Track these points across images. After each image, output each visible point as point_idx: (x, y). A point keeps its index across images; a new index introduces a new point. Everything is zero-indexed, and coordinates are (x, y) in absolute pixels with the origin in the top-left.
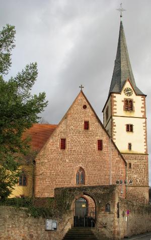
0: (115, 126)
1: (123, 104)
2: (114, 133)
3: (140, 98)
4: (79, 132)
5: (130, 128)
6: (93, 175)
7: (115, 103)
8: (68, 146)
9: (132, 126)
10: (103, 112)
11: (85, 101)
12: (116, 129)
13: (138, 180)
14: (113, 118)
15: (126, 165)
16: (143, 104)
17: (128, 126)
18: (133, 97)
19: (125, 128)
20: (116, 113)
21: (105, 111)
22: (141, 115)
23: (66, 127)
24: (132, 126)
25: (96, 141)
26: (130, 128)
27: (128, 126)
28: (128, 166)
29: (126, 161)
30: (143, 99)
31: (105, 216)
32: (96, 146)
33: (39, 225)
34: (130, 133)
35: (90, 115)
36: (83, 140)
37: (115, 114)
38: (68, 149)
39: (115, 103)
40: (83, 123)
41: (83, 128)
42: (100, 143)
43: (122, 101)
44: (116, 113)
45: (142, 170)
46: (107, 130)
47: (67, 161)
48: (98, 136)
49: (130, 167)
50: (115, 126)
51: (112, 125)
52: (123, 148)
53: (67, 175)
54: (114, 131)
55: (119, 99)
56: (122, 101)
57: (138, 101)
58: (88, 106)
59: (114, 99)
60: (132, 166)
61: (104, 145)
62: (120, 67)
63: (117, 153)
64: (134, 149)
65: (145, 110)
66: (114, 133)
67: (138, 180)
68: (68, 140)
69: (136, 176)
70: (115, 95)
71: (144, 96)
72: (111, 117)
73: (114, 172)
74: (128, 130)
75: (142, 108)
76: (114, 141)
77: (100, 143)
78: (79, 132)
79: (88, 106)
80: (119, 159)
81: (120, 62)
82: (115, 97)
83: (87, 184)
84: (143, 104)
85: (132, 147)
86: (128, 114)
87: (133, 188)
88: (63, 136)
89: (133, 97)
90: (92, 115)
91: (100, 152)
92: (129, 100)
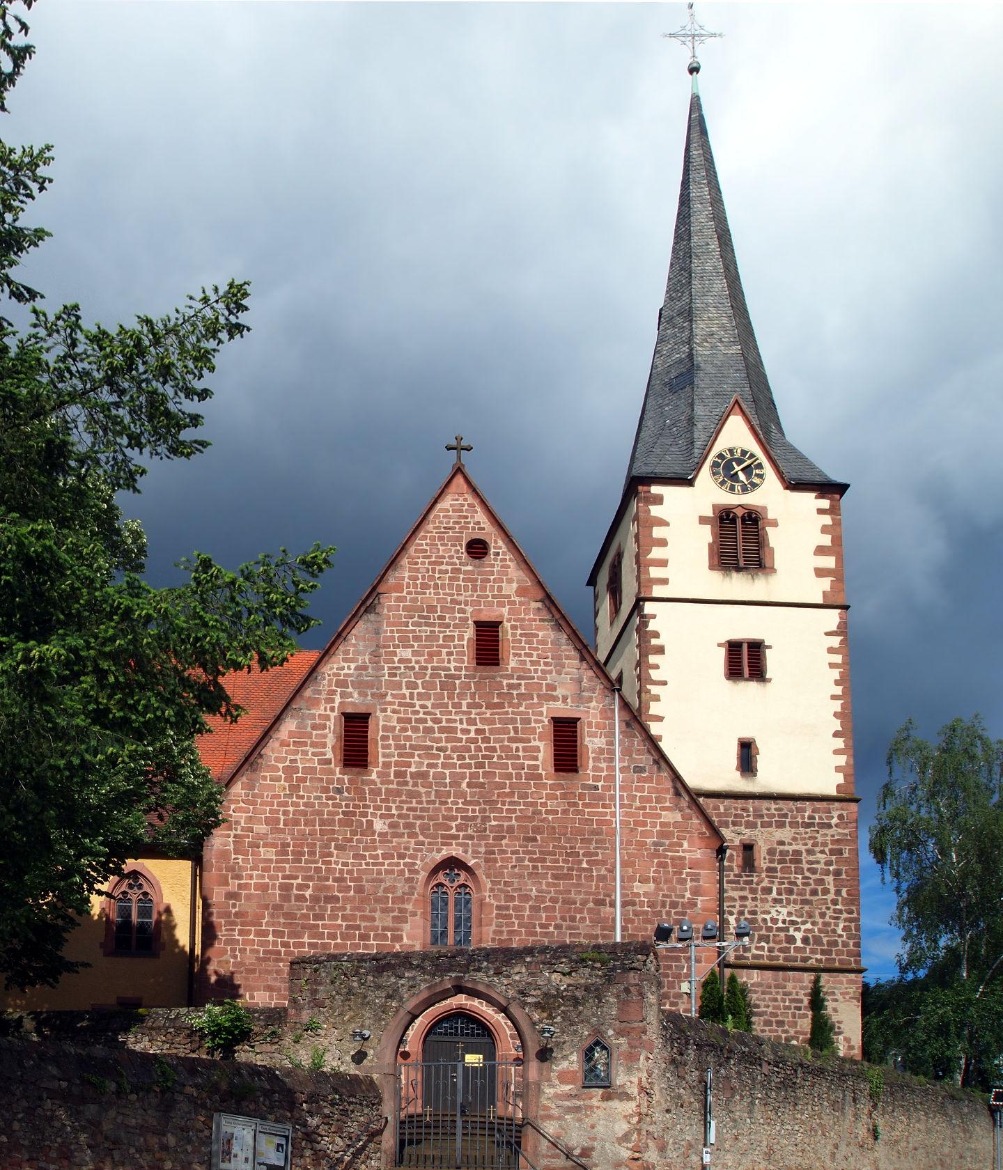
0: (660, 650)
1: (706, 535)
2: (654, 690)
3: (809, 501)
4: (447, 685)
5: (746, 661)
6: (526, 898)
7: (657, 532)
8: (382, 751)
9: (757, 648)
10: (592, 581)
11: (481, 516)
12: (663, 667)
13: (799, 936)
14: (649, 608)
15: (721, 851)
16: (825, 530)
17: (733, 648)
18: (769, 495)
19: (719, 657)
20: (664, 581)
21: (604, 578)
22: (817, 589)
23: (375, 655)
24: (757, 648)
25: (542, 724)
26: (746, 661)
27: (733, 648)
28: (734, 859)
29: (725, 832)
30: (825, 504)
31: (577, 1109)
32: (544, 751)
33: (171, 1140)
34: (750, 688)
35: (510, 589)
36: (471, 722)
37: (657, 591)
38: (387, 765)
39: (657, 532)
40: (470, 633)
41: (468, 659)
42: (565, 736)
43: (703, 520)
44: (664, 581)
45: (821, 882)
46: (614, 675)
47: (379, 825)
48: (555, 699)
49: (749, 863)
50: (660, 650)
51: (648, 646)
52: (709, 767)
53: (378, 900)
54: (654, 674)
55: (682, 516)
56: (703, 520)
57: (795, 524)
58: (497, 545)
59: (655, 511)
60: (762, 862)
61: (591, 742)
62: (690, 340)
63: (669, 785)
64: (773, 775)
65: (839, 561)
66: (654, 690)
67: (799, 936)
68: (382, 722)
69: (783, 913)
70: (655, 489)
71: (831, 489)
72: (639, 601)
73: (651, 886)
74: (734, 671)
75: (820, 550)
76: (654, 728)
77: (565, 736)
78: (447, 685)
79: (497, 545)
80: (678, 817)
81: (689, 314)
82: (659, 500)
83: (487, 935)
84: (825, 530)
85: (762, 762)
86: (738, 585)
87: (769, 974)
88: (356, 701)
89: (769, 495)
90: (521, 591)
91: (565, 780)
92: (740, 512)
